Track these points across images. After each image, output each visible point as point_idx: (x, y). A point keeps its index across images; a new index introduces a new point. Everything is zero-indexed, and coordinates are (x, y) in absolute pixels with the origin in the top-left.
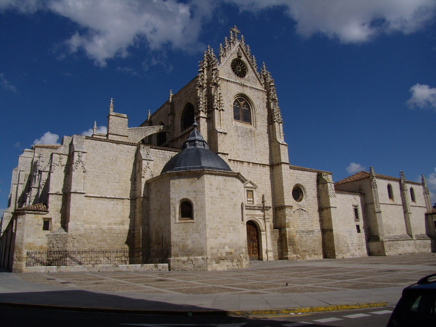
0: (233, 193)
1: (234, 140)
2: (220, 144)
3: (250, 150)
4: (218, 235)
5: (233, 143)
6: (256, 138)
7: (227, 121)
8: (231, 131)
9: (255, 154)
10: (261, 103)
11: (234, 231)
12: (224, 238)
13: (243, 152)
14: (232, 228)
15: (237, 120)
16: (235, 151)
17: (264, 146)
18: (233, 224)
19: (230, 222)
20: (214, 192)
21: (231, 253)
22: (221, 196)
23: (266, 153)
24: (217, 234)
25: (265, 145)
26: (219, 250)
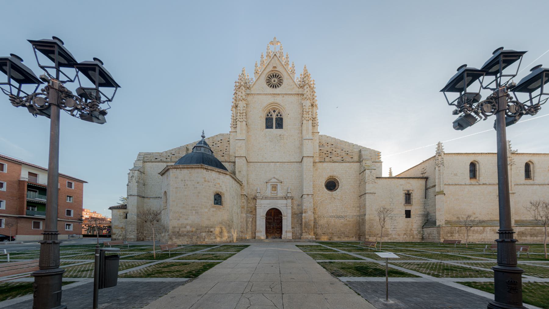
2: (237, 150)
4: (181, 217)
11: (197, 214)
12: (186, 219)
14: (194, 212)
18: (196, 208)
19: (193, 207)
20: (179, 183)
21: (192, 231)
22: (186, 186)
24: (179, 217)
26: (181, 229)
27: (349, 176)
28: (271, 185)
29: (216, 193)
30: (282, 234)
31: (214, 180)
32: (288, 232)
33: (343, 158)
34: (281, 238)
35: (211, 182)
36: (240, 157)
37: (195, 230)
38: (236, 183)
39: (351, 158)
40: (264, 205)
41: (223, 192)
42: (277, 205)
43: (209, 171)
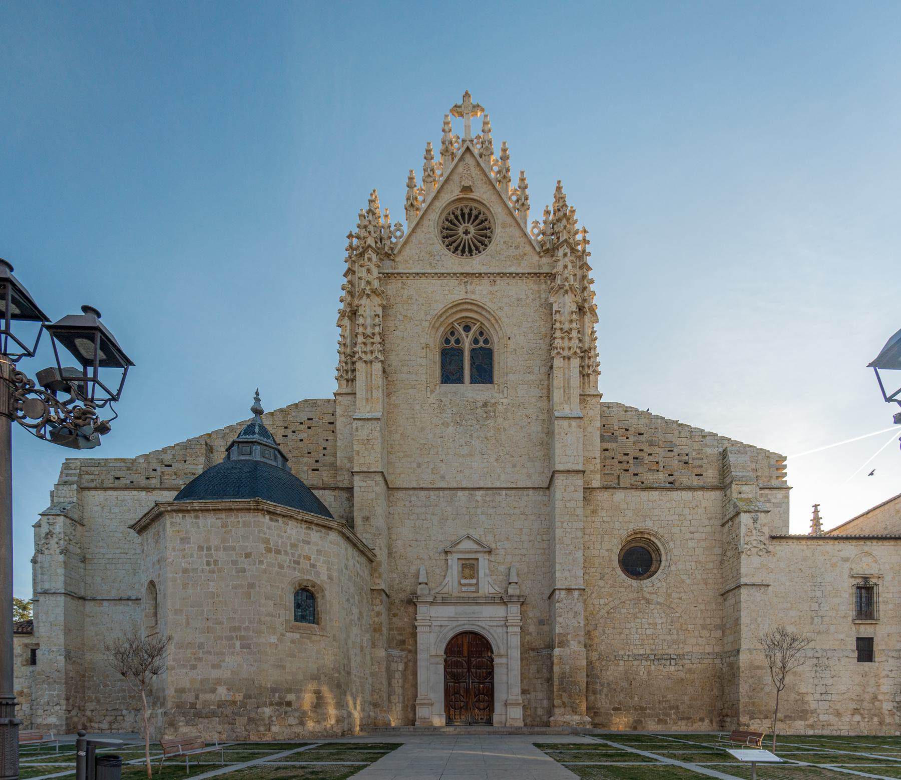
0: (248, 555)
4: (199, 659)
12: (215, 666)
14: (238, 644)
18: (243, 633)
37: (241, 698)
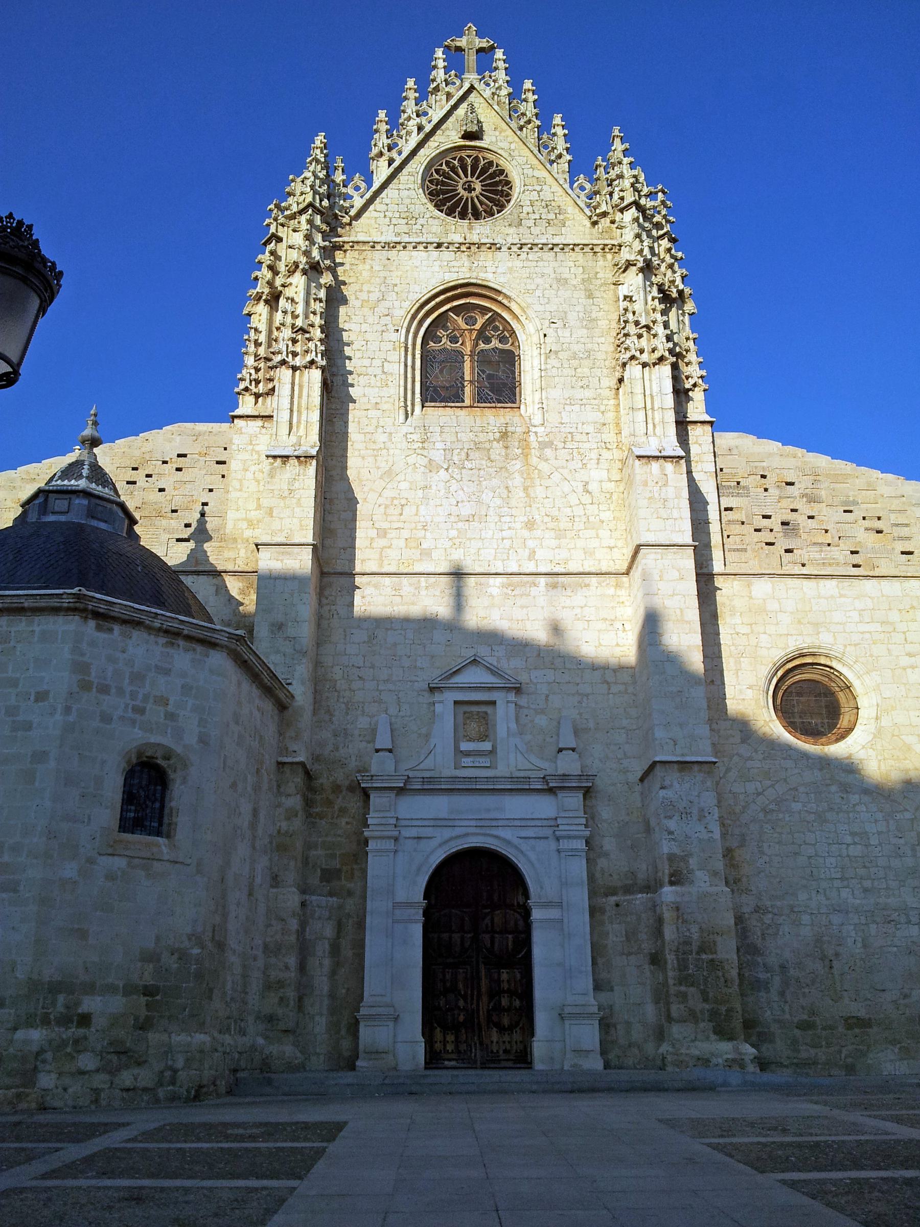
1: (404, 485)
3: (493, 518)
5: (396, 502)
6: (534, 460)
7: (372, 413)
8: (391, 452)
9: (526, 533)
10: (574, 301)
13: (453, 533)
15: (443, 404)
16: (406, 534)
17: (581, 489)
23: (592, 519)
25: (587, 483)
27: (910, 655)
28: (456, 703)
29: (140, 754)
30: (532, 1034)
31: (138, 678)
32: (574, 1016)
33: (857, 552)
34: (523, 1059)
35: (120, 691)
36: (281, 548)
38: (256, 692)
39: (903, 553)
40: (413, 832)
41: (179, 750)
42: (494, 832)
43: (111, 630)
